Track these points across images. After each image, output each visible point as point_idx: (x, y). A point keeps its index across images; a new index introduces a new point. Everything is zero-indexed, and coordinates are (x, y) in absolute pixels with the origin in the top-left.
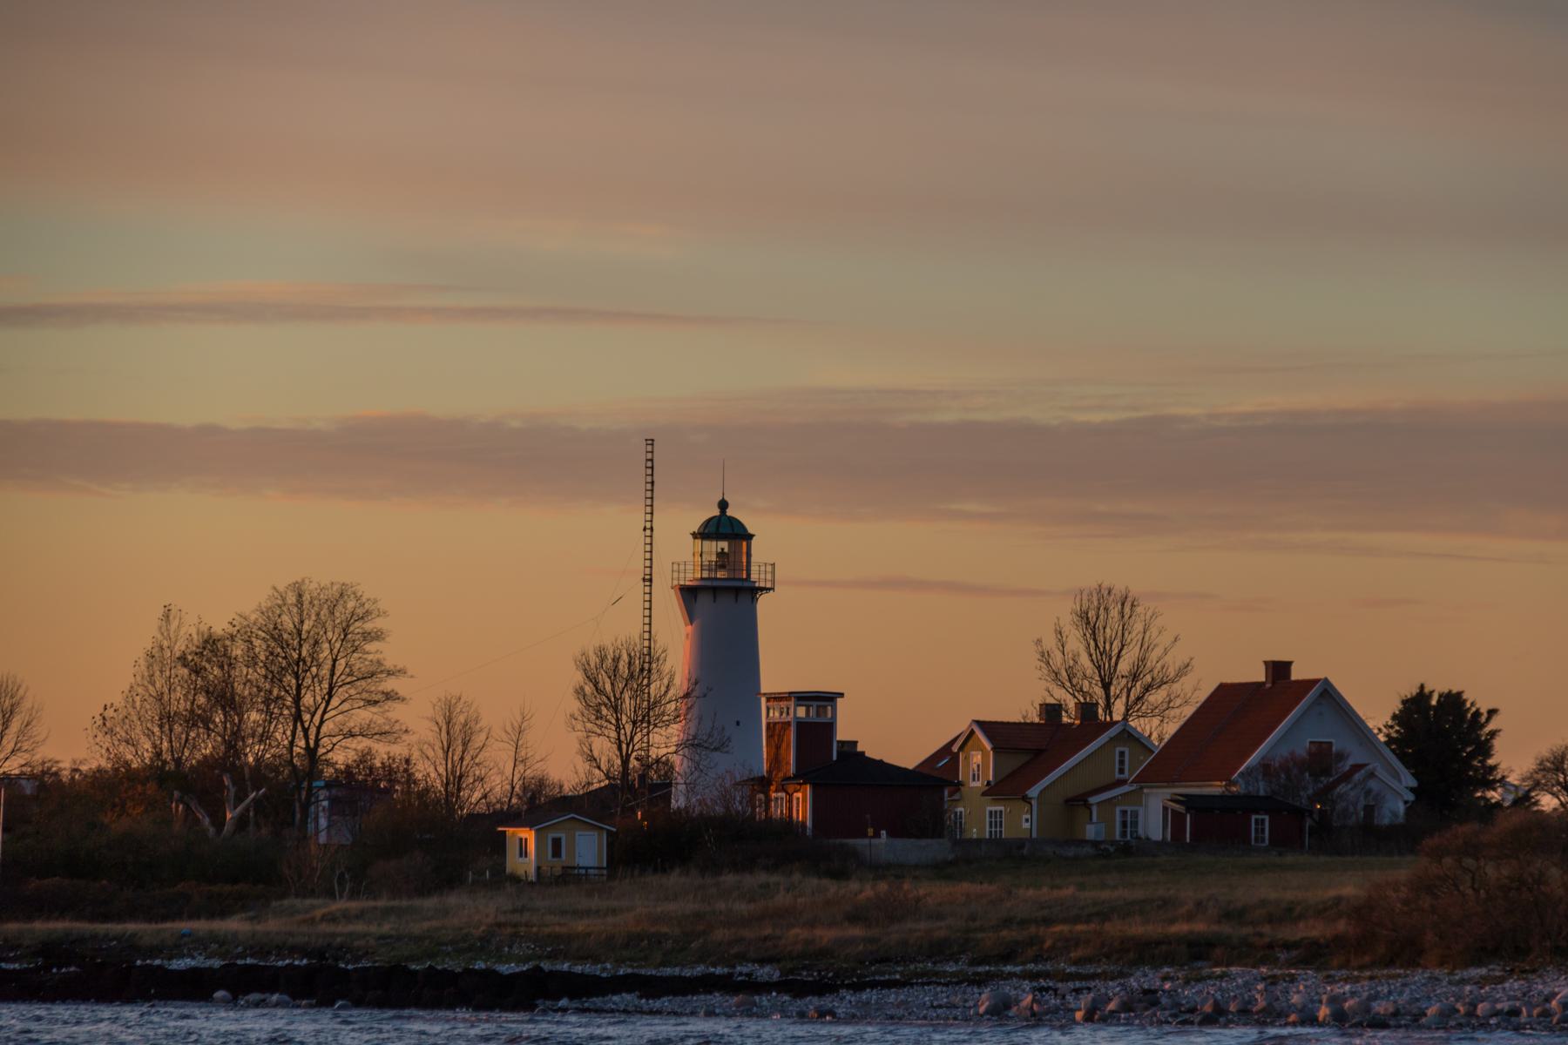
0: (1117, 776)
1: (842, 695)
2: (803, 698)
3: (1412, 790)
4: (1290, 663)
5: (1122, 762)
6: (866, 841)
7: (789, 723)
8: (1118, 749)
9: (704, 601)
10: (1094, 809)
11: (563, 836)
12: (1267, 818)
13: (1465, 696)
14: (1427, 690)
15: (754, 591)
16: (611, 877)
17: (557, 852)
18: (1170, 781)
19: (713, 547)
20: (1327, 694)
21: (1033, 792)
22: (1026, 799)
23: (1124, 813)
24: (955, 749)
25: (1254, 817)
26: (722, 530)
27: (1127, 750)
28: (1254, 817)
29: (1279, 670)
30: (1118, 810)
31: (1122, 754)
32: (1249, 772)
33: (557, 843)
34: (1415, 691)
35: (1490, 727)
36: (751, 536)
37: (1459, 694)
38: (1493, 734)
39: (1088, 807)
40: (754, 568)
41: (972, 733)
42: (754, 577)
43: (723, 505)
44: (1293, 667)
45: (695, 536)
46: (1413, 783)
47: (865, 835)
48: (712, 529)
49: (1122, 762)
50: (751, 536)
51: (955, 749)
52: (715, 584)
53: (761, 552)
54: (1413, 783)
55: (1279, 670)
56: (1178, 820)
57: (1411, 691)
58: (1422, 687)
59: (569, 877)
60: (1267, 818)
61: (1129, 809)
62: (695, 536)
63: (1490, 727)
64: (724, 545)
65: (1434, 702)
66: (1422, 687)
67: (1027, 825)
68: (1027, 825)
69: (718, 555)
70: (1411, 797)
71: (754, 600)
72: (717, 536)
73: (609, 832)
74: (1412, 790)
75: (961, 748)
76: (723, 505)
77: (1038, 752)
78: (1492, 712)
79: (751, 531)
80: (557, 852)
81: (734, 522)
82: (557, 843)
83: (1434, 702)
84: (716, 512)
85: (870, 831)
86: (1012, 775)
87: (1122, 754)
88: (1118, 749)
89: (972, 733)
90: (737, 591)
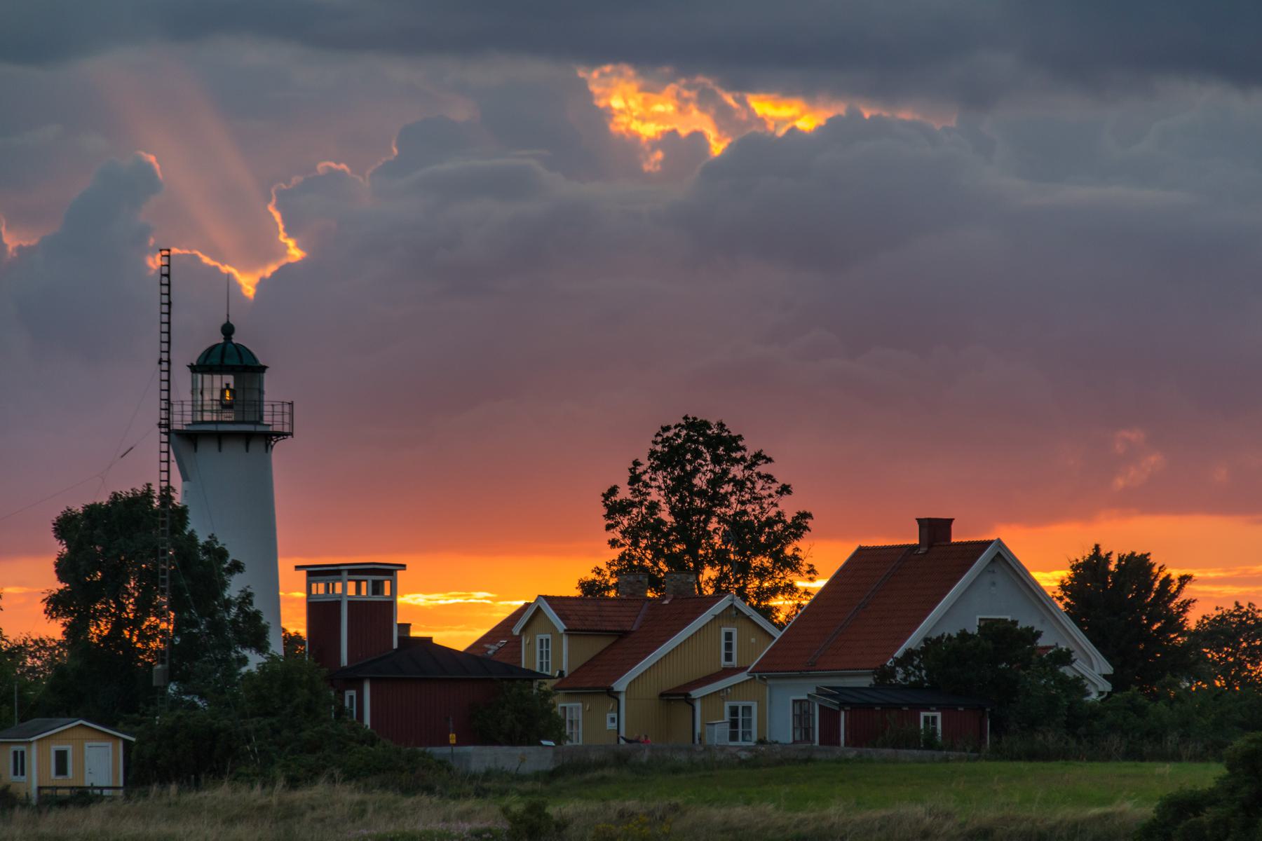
0: (724, 663)
1: (403, 567)
2: (357, 571)
3: (1106, 677)
4: (949, 522)
5: (729, 646)
6: (447, 750)
7: (337, 604)
8: (724, 630)
9: (207, 451)
10: (698, 705)
11: (69, 748)
12: (939, 715)
13: (1152, 559)
14: (1103, 553)
15: (268, 438)
16: (128, 797)
17: (61, 769)
18: (804, 672)
19: (216, 384)
20: (1004, 561)
21: (621, 685)
22: (614, 695)
23: (734, 711)
24: (516, 631)
25: (923, 714)
26: (227, 362)
27: (735, 631)
28: (923, 714)
29: (936, 529)
30: (727, 705)
31: (729, 636)
32: (909, 654)
33: (61, 757)
34: (1088, 552)
35: (1184, 596)
36: (263, 369)
37: (1144, 557)
38: (1186, 605)
39: (690, 702)
40: (267, 409)
41: (539, 609)
42: (267, 419)
43: (228, 330)
44: (954, 527)
45: (194, 369)
46: (1109, 670)
47: (446, 743)
48: (215, 360)
49: (729, 646)
50: (263, 369)
51: (516, 631)
52: (221, 428)
53: (273, 389)
54: (1109, 670)
55: (936, 529)
56: (829, 717)
57: (1083, 553)
58: (1097, 547)
59: (84, 797)
60: (939, 715)
61: (740, 704)
62: (194, 369)
63: (1184, 596)
64: (230, 379)
65: (1112, 567)
66: (1097, 547)
67: (613, 726)
68: (611, 726)
69: (223, 392)
70: (1108, 687)
71: (268, 447)
72: (221, 369)
73: (126, 742)
74: (1106, 677)
75: (524, 629)
76: (228, 330)
77: (622, 635)
78: (1184, 579)
79: (262, 363)
80: (61, 769)
81: (241, 351)
82: (61, 757)
83: (1112, 567)
84: (220, 339)
85: (453, 738)
86: (590, 664)
87: (729, 636)
88: (724, 630)
89: (539, 609)
90: (248, 437)
